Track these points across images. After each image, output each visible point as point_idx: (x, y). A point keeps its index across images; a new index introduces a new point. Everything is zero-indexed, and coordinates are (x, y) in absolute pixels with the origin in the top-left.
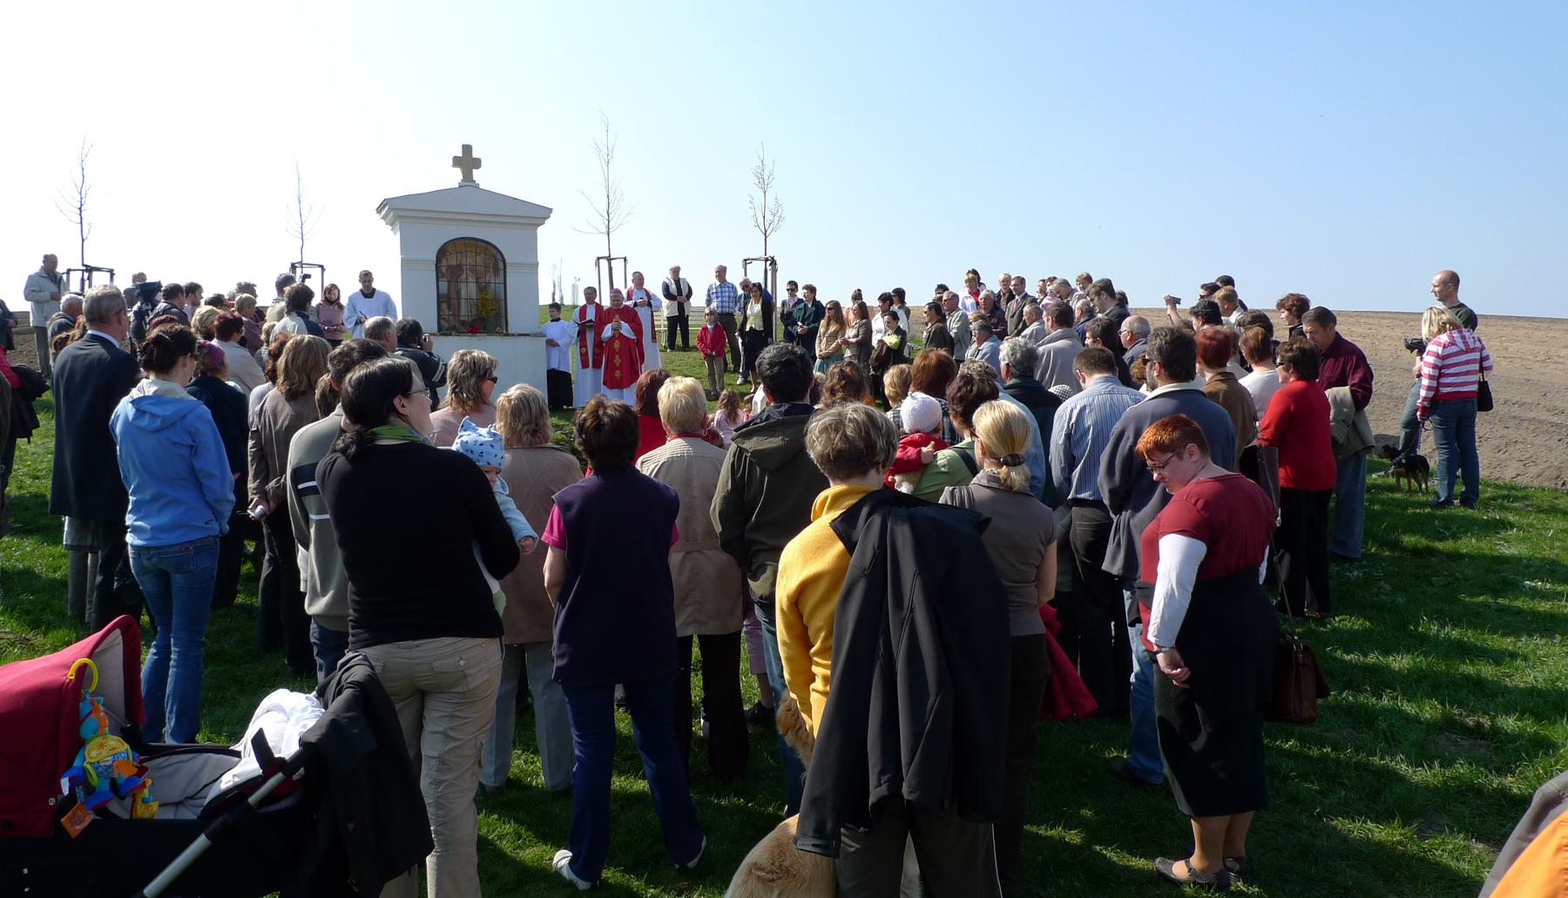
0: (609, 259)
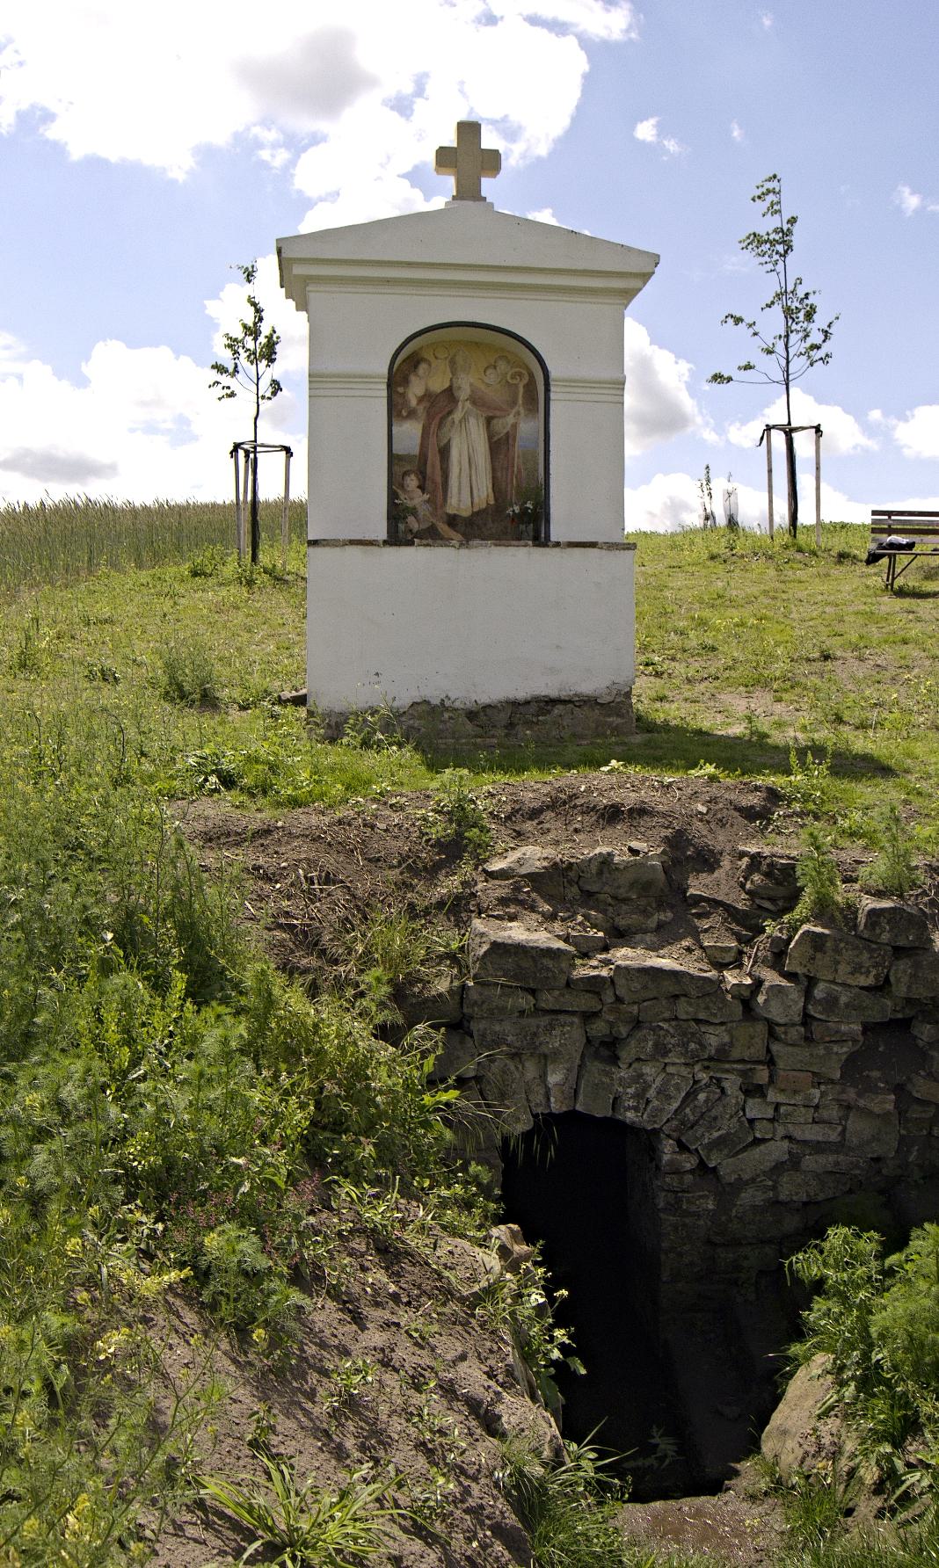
0: (789, 431)
